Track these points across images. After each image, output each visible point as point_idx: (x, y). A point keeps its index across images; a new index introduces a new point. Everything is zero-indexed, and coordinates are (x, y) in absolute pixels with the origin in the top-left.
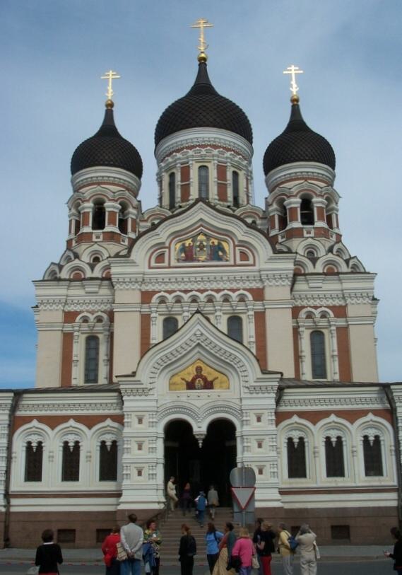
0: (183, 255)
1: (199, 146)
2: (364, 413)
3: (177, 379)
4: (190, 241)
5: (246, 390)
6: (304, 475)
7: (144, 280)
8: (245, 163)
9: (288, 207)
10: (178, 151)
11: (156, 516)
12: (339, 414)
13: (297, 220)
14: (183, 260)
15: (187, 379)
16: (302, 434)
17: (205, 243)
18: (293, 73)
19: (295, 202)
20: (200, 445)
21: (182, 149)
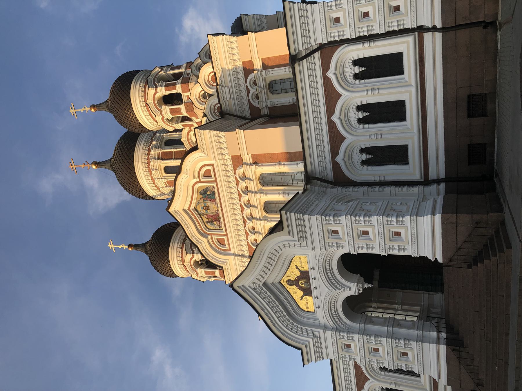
0: (215, 223)
1: (151, 174)
2: (327, 81)
3: (302, 304)
4: (203, 217)
5: (304, 243)
6: (405, 148)
7: (240, 256)
8: (158, 135)
9: (172, 116)
10: (158, 189)
11: (454, 350)
12: (330, 111)
13: (180, 108)
14: (220, 223)
15: (302, 295)
16: (357, 152)
17: (203, 206)
18: (74, 111)
19: (166, 109)
20: (370, 286)
21: (156, 186)
